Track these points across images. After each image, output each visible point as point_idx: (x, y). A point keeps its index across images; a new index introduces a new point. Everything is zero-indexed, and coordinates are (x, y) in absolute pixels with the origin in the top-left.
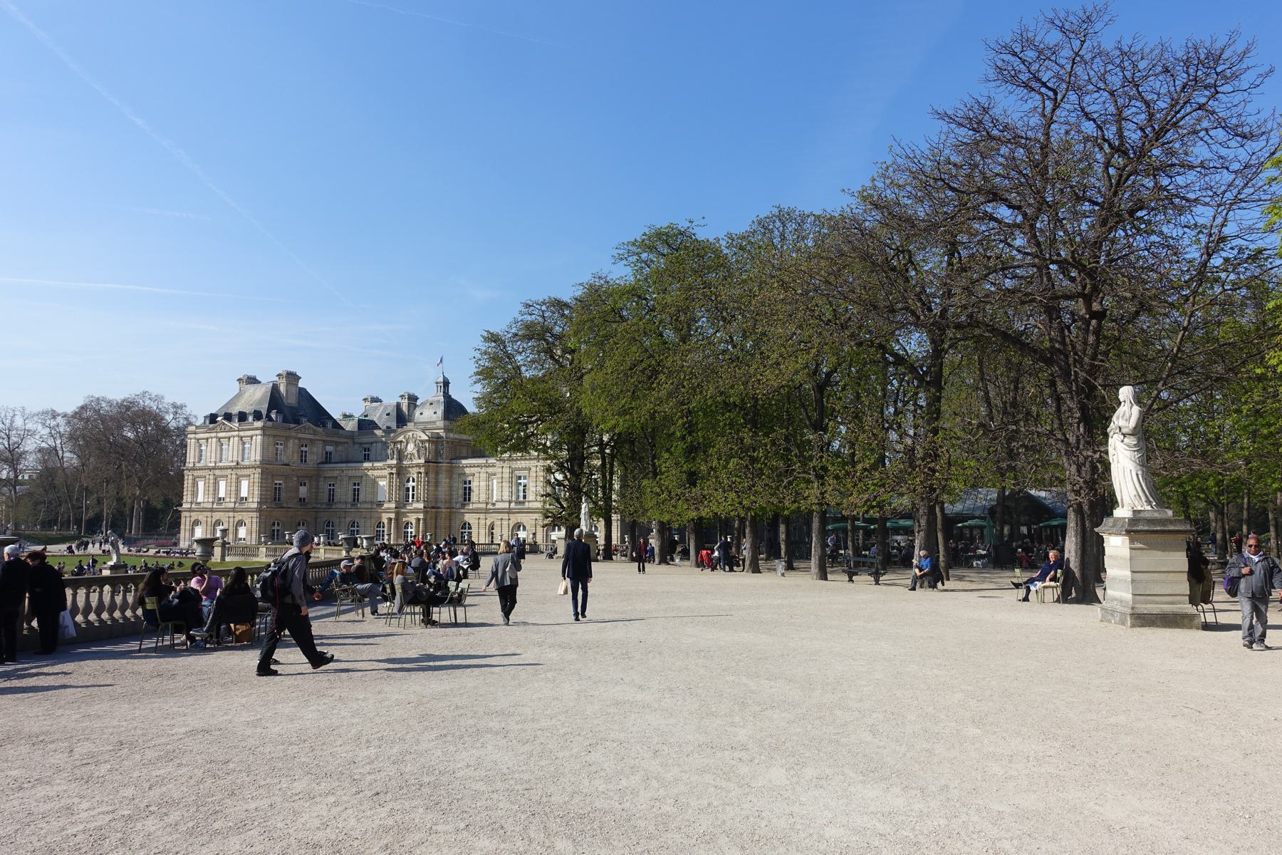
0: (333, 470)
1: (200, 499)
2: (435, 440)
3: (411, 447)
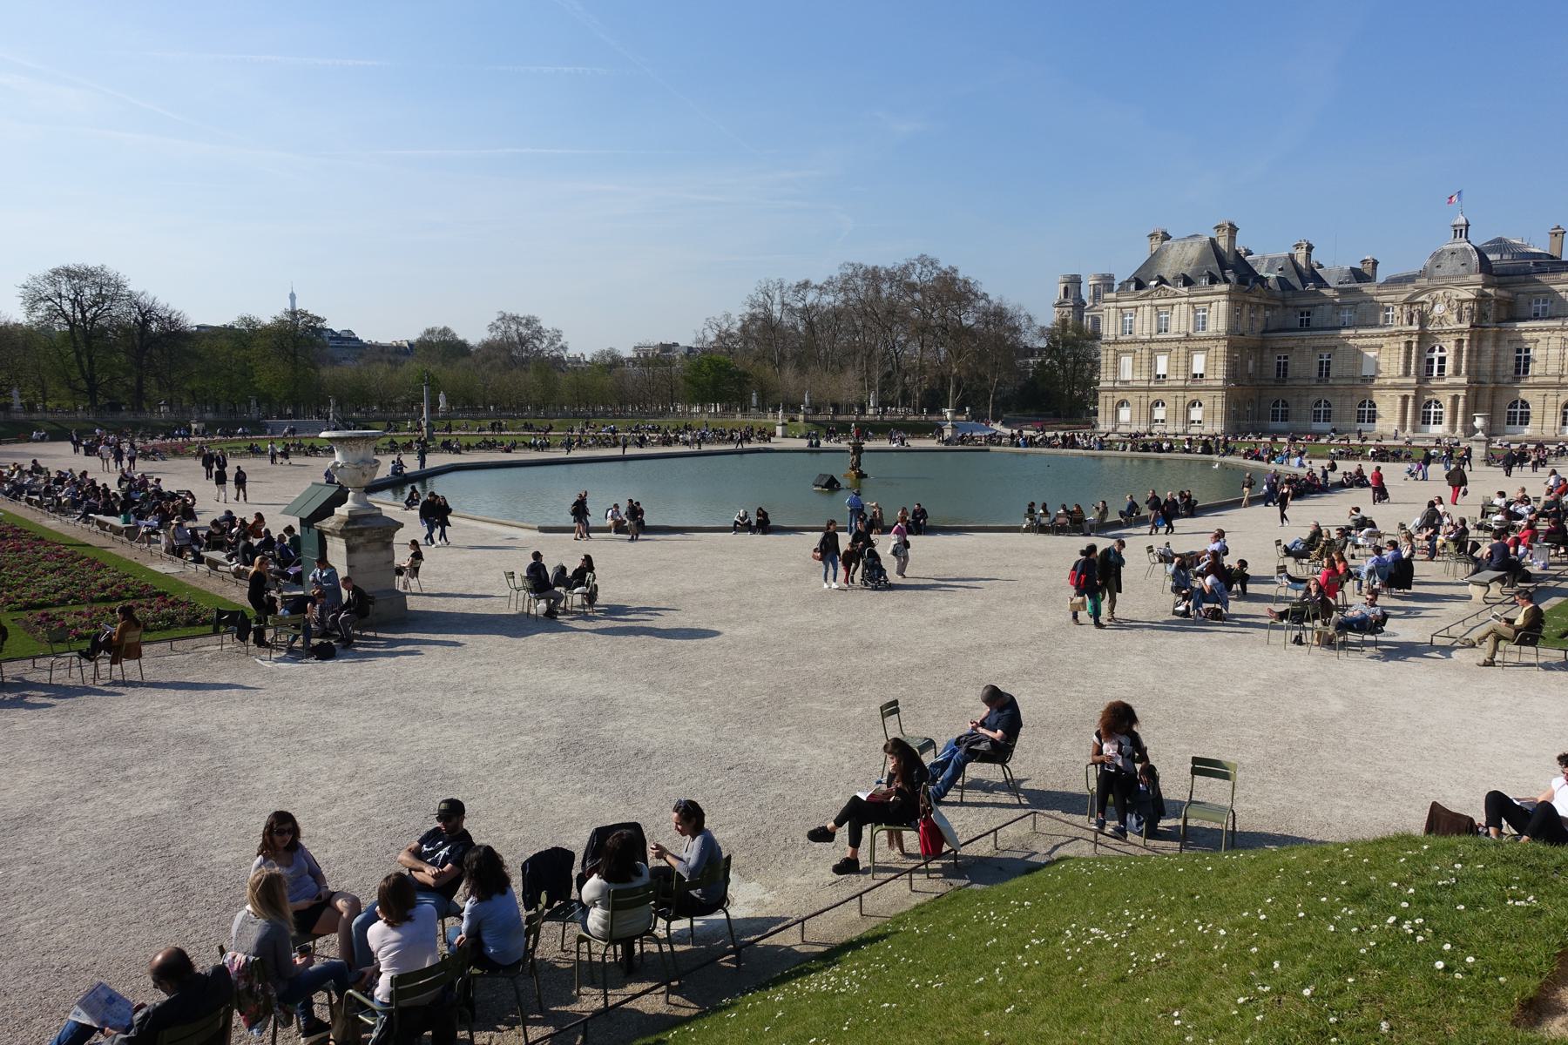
0: (1291, 340)
1: (1127, 374)
2: (1481, 299)
3: (1439, 309)
